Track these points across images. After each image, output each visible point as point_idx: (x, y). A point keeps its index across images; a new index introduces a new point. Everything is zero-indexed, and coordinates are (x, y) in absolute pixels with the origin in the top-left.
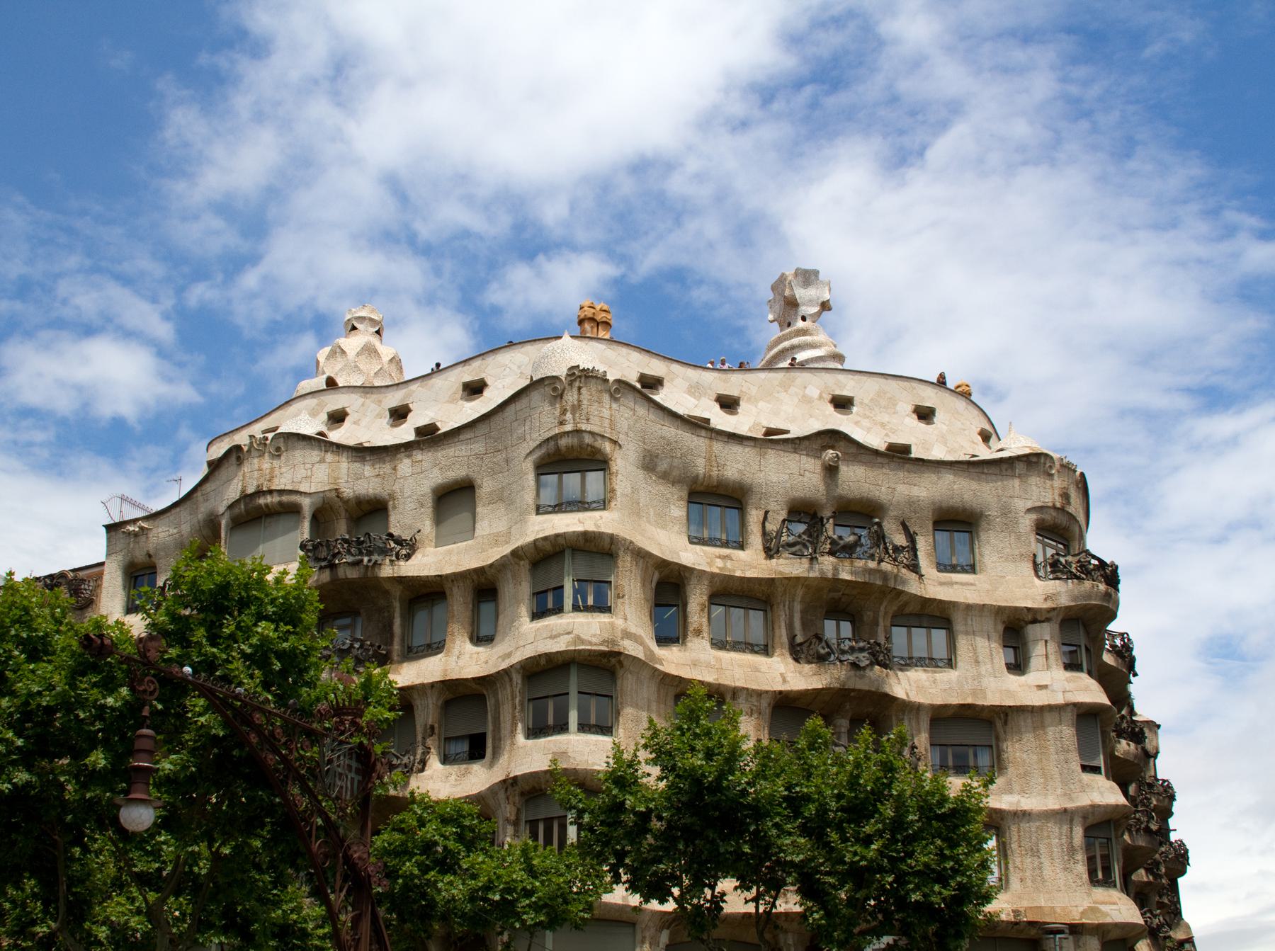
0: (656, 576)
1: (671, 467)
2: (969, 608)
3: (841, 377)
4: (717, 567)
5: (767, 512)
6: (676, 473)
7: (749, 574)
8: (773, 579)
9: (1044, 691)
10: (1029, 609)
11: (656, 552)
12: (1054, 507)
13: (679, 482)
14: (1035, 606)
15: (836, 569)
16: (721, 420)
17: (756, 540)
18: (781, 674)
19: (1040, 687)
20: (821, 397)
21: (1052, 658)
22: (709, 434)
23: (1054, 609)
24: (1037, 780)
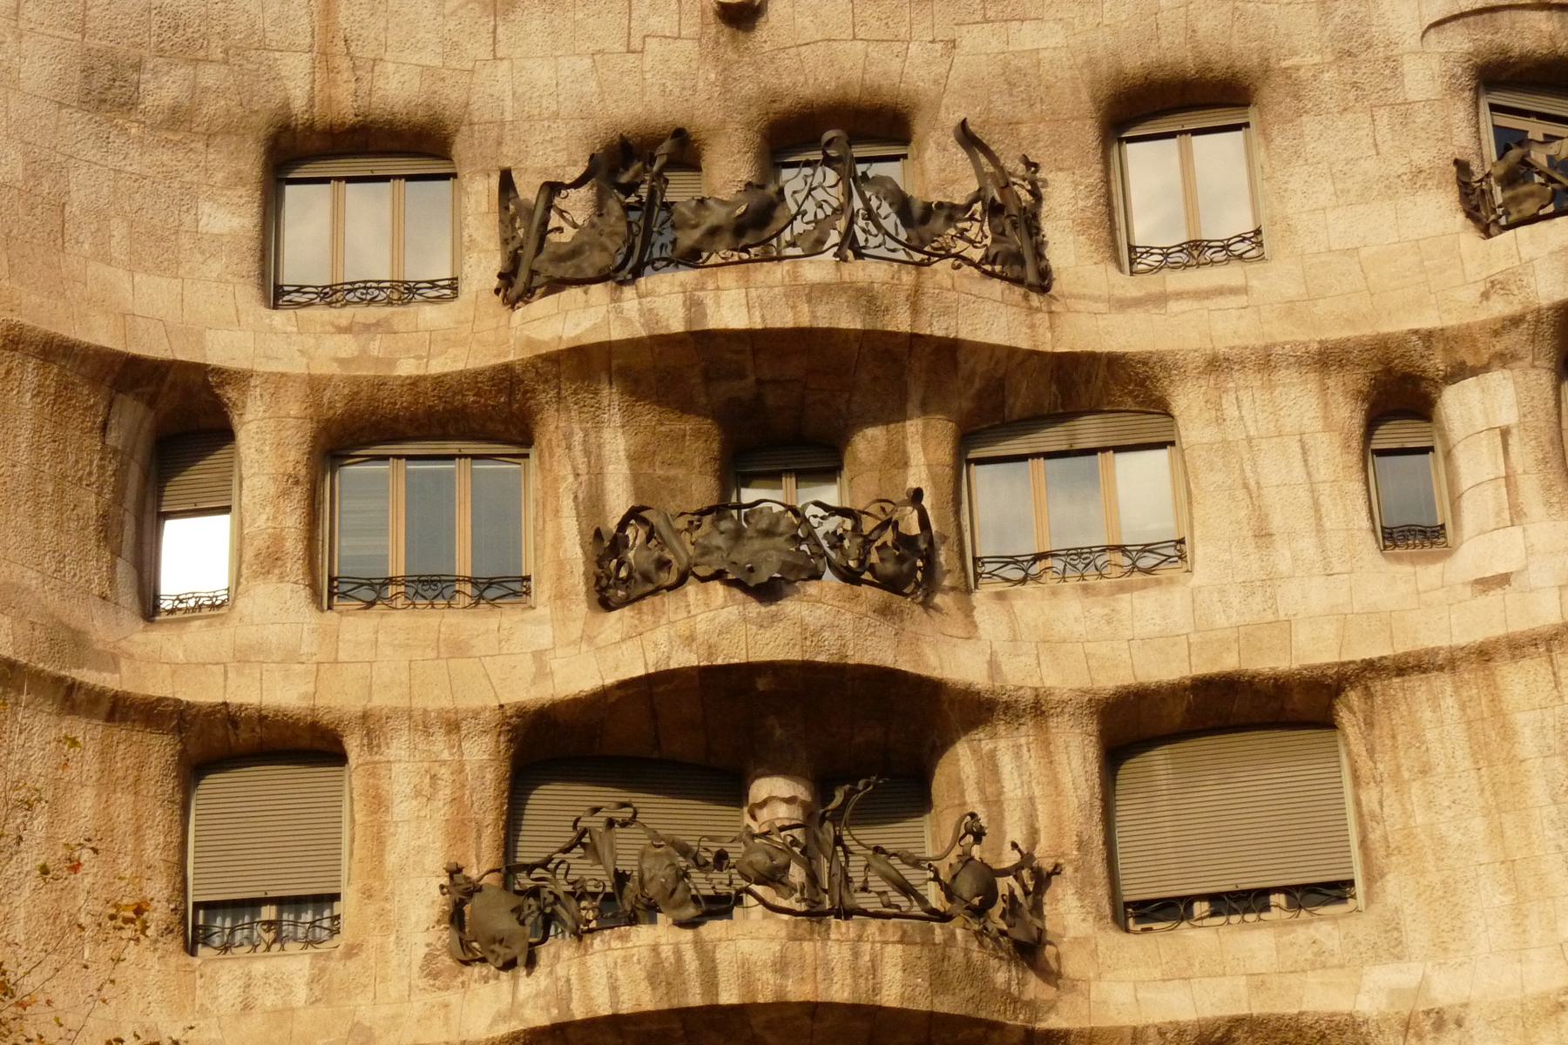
0: (131, 420)
2: (1216, 365)
6: (212, 108)
7: (437, 367)
8: (507, 368)
9: (1495, 596)
10: (1428, 337)
11: (102, 334)
13: (227, 130)
14: (1451, 321)
15: (694, 305)
18: (538, 656)
19: (1486, 584)
21: (1530, 488)
23: (1515, 321)
24: (1488, 901)
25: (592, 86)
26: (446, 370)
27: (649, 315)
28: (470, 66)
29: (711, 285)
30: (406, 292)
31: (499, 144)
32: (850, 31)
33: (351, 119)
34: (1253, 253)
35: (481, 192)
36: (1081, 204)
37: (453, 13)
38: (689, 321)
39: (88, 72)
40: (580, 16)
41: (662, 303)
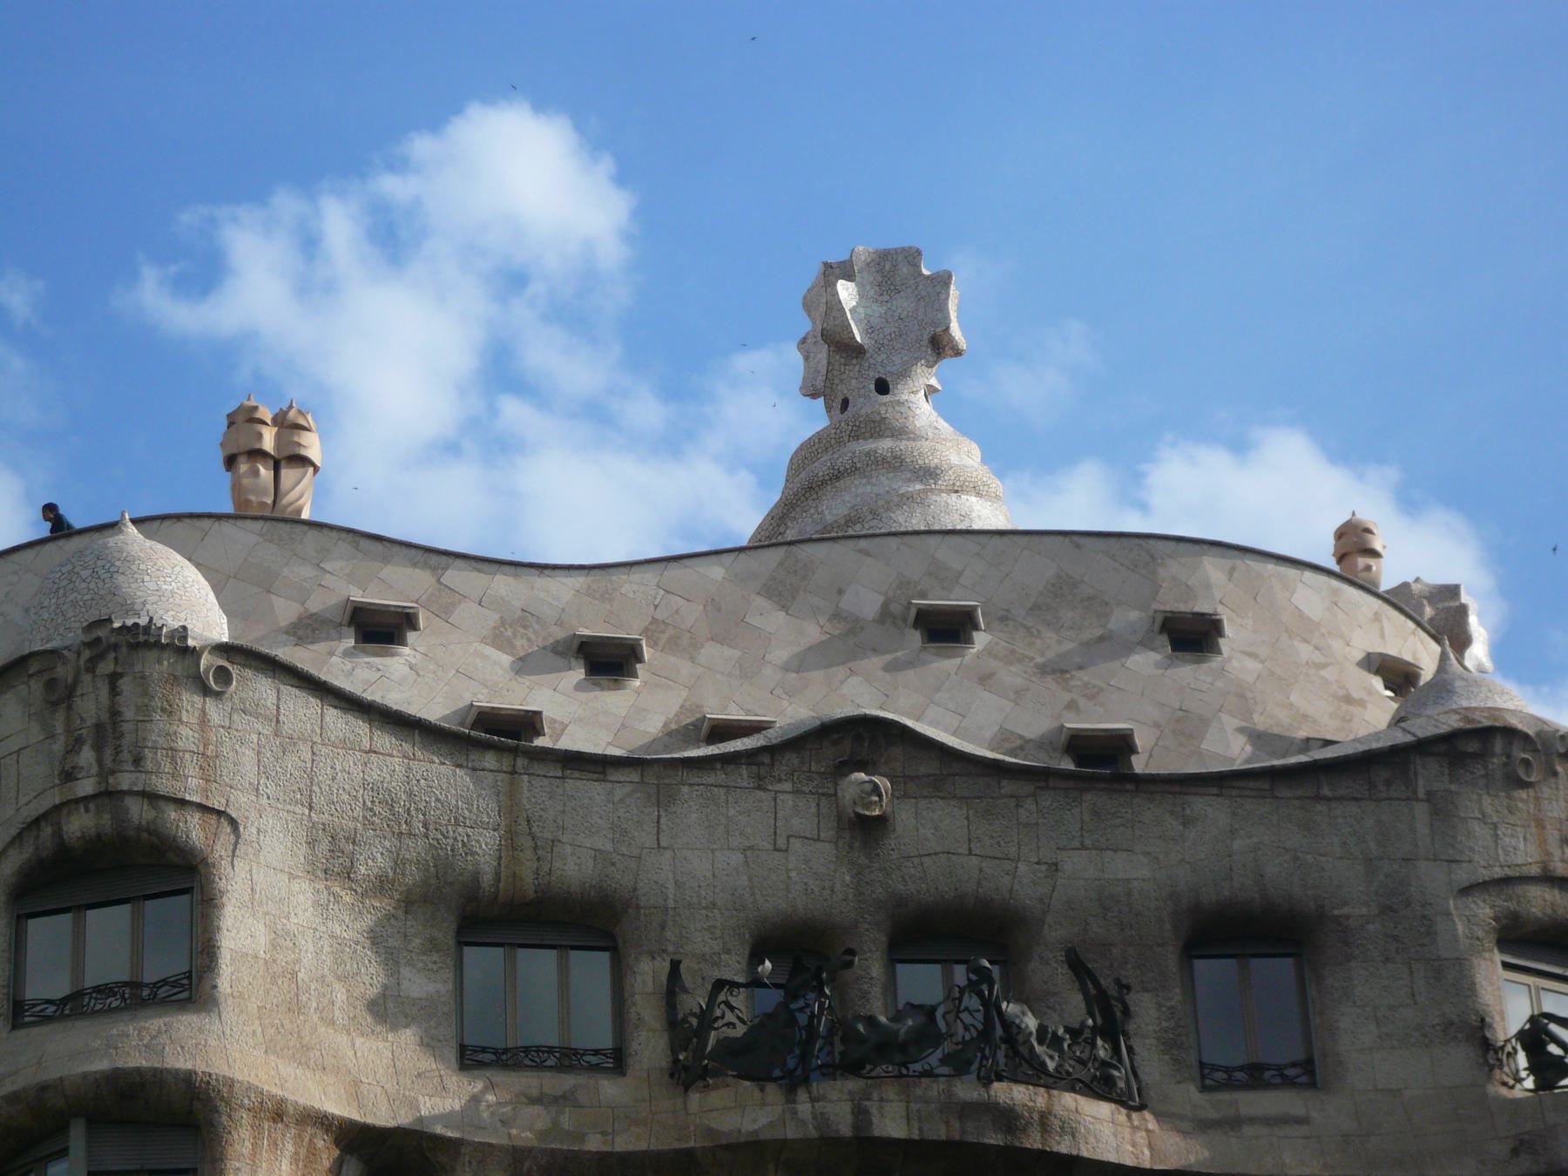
1: (398, 862)
3: (945, 551)
4: (528, 1128)
5: (675, 966)
6: (412, 875)
7: (625, 1142)
8: (689, 1152)
12: (1549, 879)
15: (861, 1115)
16: (578, 716)
17: (650, 1047)
20: (885, 615)
22: (506, 763)
25: (744, 880)
26: (631, 1148)
27: (821, 1120)
28: (636, 852)
29: (875, 1096)
30: (568, 1059)
31: (663, 928)
32: (966, 846)
33: (532, 895)
34: (1304, 1079)
35: (647, 974)
36: (1165, 1024)
37: (622, 801)
38: (855, 1126)
39: (312, 843)
40: (732, 812)
41: (832, 1105)
